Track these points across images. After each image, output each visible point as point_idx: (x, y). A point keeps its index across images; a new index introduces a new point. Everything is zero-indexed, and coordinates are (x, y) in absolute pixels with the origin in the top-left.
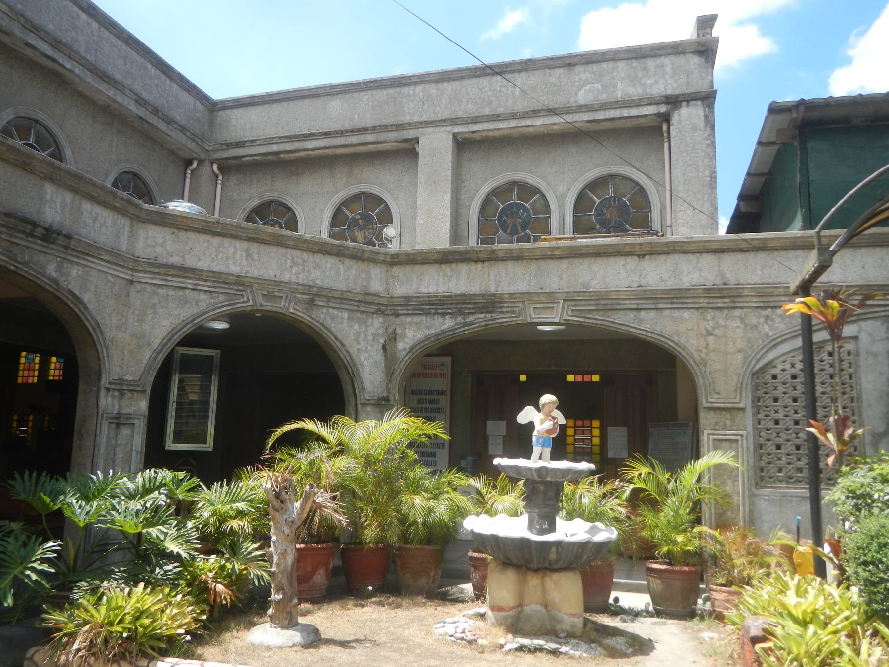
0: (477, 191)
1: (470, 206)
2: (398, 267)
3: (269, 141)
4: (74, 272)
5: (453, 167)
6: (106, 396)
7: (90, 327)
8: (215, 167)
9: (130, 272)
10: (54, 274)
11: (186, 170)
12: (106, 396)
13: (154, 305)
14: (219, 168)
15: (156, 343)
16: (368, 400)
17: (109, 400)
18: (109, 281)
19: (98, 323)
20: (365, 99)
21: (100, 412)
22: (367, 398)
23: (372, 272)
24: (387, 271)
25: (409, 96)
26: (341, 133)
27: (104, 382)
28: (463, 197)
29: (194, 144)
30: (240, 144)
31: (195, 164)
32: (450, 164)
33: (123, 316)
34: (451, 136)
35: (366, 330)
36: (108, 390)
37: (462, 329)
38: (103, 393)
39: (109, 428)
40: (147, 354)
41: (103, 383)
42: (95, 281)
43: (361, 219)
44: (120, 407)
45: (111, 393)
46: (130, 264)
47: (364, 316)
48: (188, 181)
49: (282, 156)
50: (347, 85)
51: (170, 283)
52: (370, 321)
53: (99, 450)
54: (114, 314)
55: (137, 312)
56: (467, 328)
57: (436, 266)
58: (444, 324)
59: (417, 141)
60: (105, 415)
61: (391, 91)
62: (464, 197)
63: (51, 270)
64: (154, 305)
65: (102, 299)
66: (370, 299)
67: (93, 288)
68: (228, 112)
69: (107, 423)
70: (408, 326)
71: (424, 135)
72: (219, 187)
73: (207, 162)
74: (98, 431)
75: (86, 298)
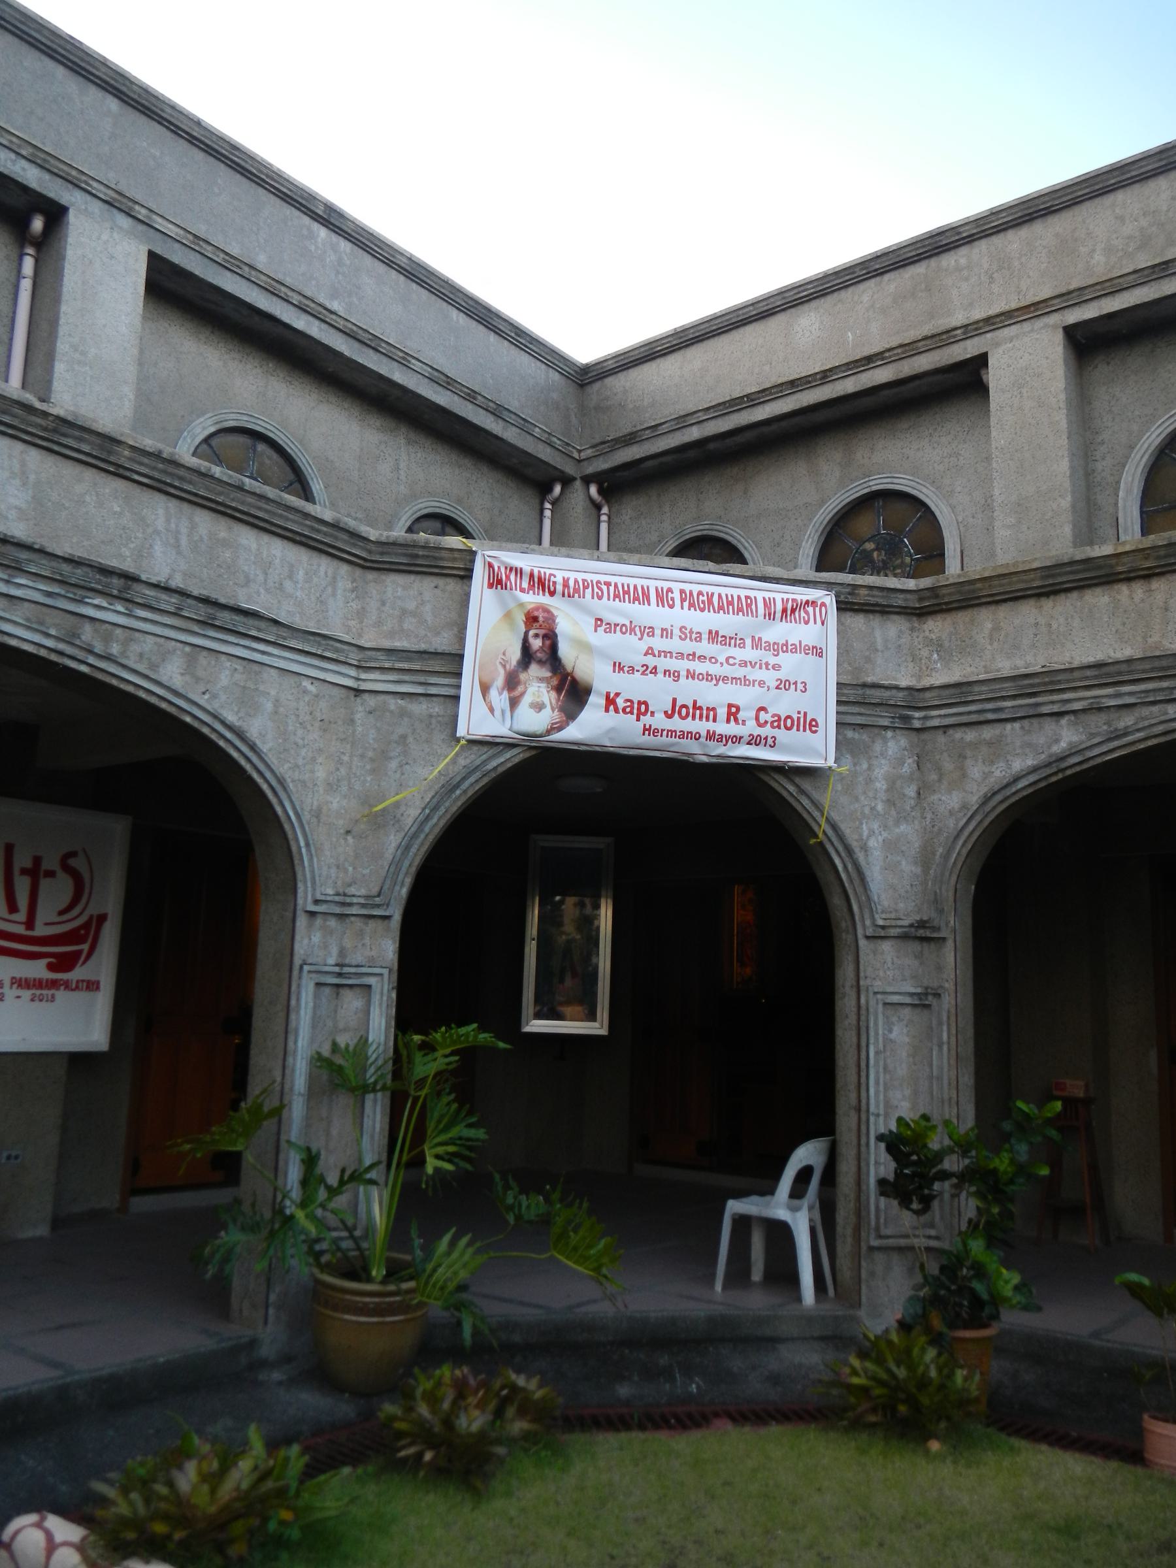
0: (1132, 448)
1: (1118, 482)
2: (939, 617)
3: (683, 421)
4: (226, 676)
5: (1069, 402)
6: (310, 926)
7: (265, 787)
8: (593, 490)
9: (353, 672)
10: (178, 682)
11: (542, 504)
12: (310, 926)
13: (404, 737)
14: (600, 492)
15: (412, 814)
16: (883, 927)
17: (317, 938)
18: (305, 692)
19: (281, 782)
20: (866, 298)
21: (297, 962)
22: (881, 923)
23: (878, 634)
24: (912, 629)
25: (959, 269)
26: (824, 377)
27: (305, 899)
28: (1099, 466)
29: (549, 450)
30: (630, 439)
31: (557, 489)
32: (1063, 396)
33: (340, 762)
34: (1059, 337)
35: (870, 768)
36: (312, 914)
37: (1104, 748)
38: (302, 921)
39: (316, 996)
40: (392, 841)
41: (300, 901)
42: (273, 692)
43: (877, 549)
44: (342, 952)
45: (319, 921)
46: (351, 655)
47: (864, 736)
48: (547, 523)
49: (711, 446)
50: (826, 277)
51: (433, 690)
52: (878, 747)
53: (296, 1042)
54: (320, 760)
55: (370, 754)
56: (1116, 743)
57: (1032, 602)
58: (1057, 741)
59: (982, 360)
60: (306, 968)
61: (919, 269)
62: (1103, 466)
63: (173, 673)
64: (404, 737)
65: (291, 728)
66: (876, 695)
67: (269, 706)
68: (609, 381)
69: (311, 986)
70: (969, 753)
71: (997, 345)
72: (604, 527)
73: (578, 484)
74: (293, 1002)
75: (255, 728)
